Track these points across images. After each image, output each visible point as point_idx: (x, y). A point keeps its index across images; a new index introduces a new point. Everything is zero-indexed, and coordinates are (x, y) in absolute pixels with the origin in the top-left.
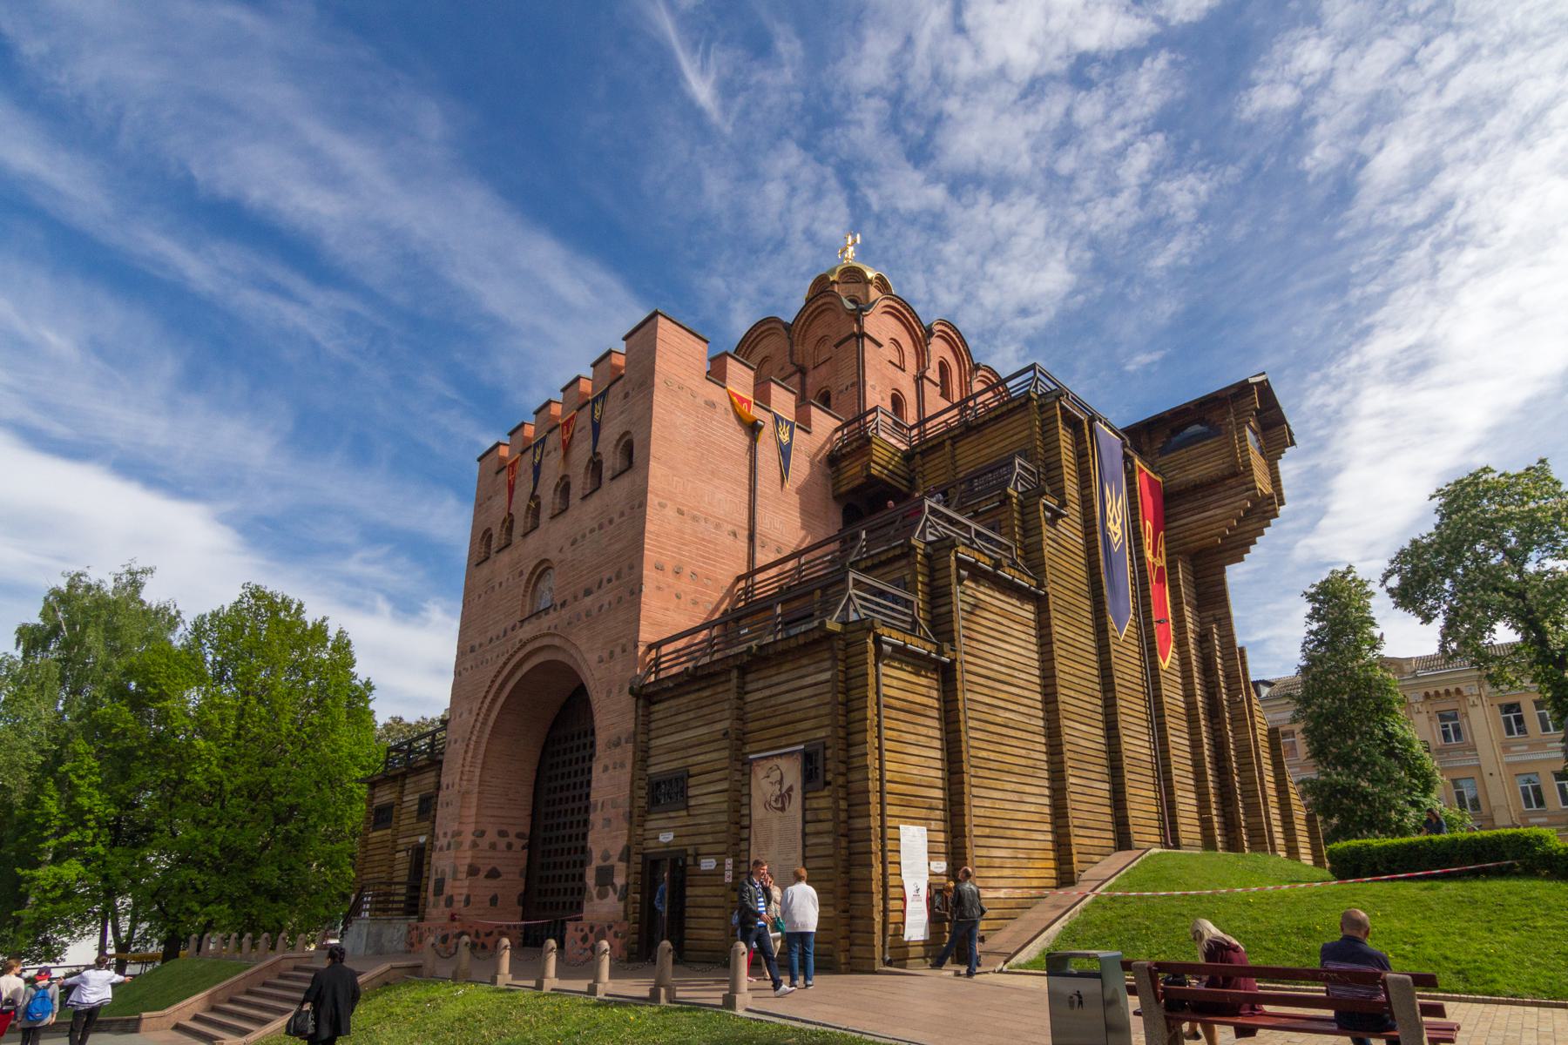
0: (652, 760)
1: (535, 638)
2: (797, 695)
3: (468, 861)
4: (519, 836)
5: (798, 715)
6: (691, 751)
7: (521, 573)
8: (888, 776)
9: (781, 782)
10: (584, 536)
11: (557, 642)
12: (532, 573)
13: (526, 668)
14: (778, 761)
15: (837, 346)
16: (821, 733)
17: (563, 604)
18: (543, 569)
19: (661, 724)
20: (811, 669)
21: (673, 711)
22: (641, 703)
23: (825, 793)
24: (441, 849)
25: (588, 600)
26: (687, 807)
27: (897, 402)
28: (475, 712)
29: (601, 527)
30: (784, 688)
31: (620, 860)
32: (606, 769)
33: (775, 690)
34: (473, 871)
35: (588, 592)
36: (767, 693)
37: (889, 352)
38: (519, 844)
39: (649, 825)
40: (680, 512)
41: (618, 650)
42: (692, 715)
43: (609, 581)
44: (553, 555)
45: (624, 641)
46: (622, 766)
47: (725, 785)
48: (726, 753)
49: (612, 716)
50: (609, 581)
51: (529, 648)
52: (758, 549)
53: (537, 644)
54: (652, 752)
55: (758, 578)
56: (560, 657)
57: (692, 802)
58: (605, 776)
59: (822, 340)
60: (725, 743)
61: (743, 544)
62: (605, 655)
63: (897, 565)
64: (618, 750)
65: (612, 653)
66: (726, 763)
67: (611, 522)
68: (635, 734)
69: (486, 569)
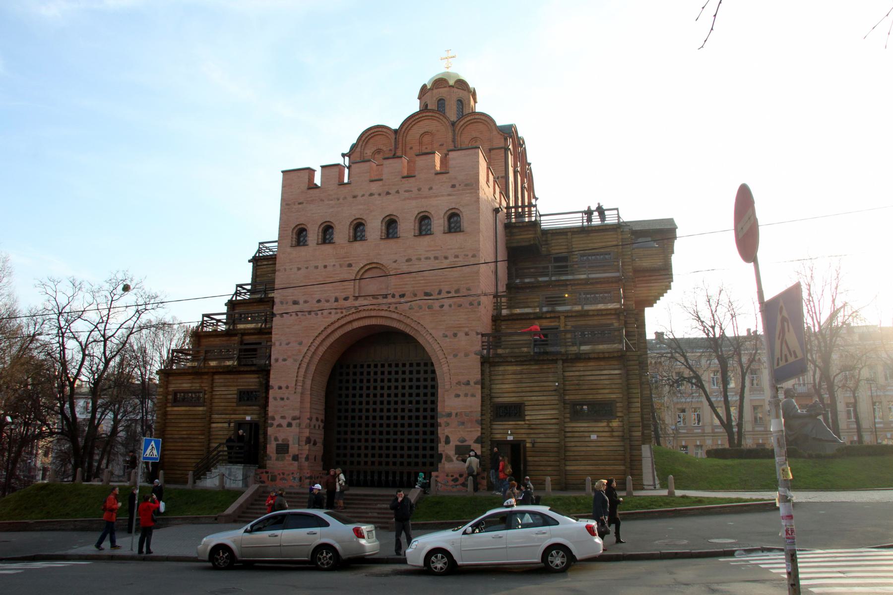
2: (597, 378)
3: (308, 435)
4: (322, 421)
5: (599, 387)
7: (350, 265)
13: (356, 325)
24: (280, 426)
26: (524, 420)
31: (476, 441)
34: (308, 441)
38: (322, 425)
39: (495, 427)
42: (524, 376)
45: (467, 330)
46: (473, 395)
48: (556, 398)
57: (527, 418)
64: (468, 387)
65: (455, 335)
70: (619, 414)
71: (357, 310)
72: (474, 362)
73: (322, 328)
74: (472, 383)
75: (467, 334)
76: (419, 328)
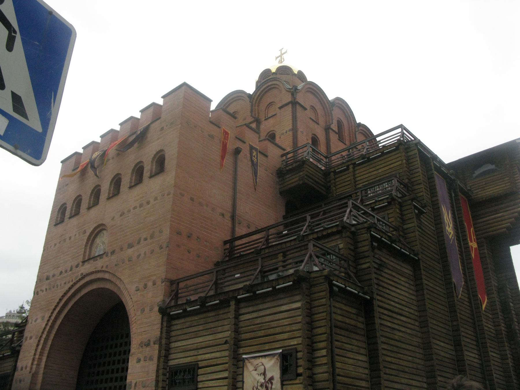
0: (172, 356)
1: (92, 273)
5: (278, 330)
6: (201, 351)
7: (85, 232)
8: (337, 371)
9: (264, 374)
10: (129, 211)
11: (107, 276)
12: (92, 232)
14: (263, 360)
15: (280, 108)
16: (294, 342)
17: (113, 253)
18: (99, 229)
19: (179, 332)
20: (287, 300)
21: (188, 324)
22: (165, 319)
23: (297, 381)
25: (130, 251)
27: (315, 141)
28: (46, 318)
29: (141, 206)
30: (268, 312)
32: (139, 361)
33: (261, 313)
35: (130, 246)
36: (255, 315)
37: (309, 113)
40: (192, 199)
41: (150, 284)
42: (201, 327)
43: (146, 239)
44: (107, 221)
46: (151, 359)
47: (225, 374)
48: (226, 353)
49: (144, 326)
50: (146, 239)
51: (87, 279)
52: (237, 225)
53: (93, 277)
54: (172, 351)
55: (237, 243)
56: (108, 286)
58: (138, 365)
59: (271, 104)
60: (226, 346)
61: (227, 221)
62: (141, 286)
63: (333, 238)
64: (148, 349)
65: (145, 286)
66: (226, 359)
67: (148, 203)
68: (161, 338)
69: (61, 228)
70: (300, 370)
71: (83, 277)
72: (156, 318)
73: (58, 300)
74: (152, 343)
75: (154, 284)
76: (121, 286)
